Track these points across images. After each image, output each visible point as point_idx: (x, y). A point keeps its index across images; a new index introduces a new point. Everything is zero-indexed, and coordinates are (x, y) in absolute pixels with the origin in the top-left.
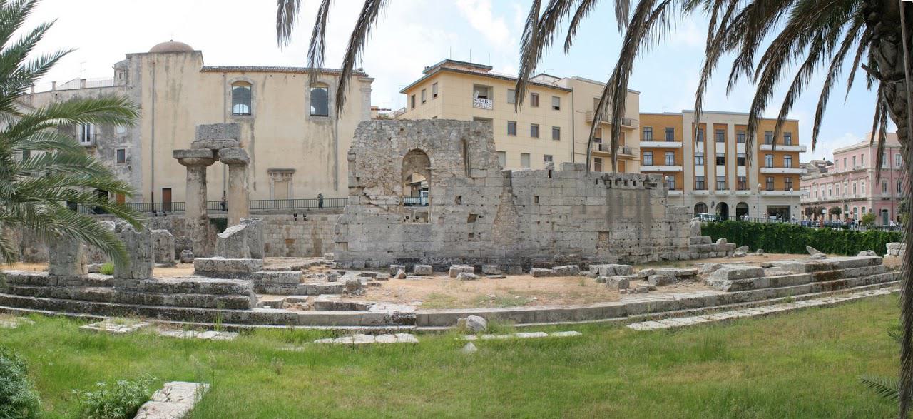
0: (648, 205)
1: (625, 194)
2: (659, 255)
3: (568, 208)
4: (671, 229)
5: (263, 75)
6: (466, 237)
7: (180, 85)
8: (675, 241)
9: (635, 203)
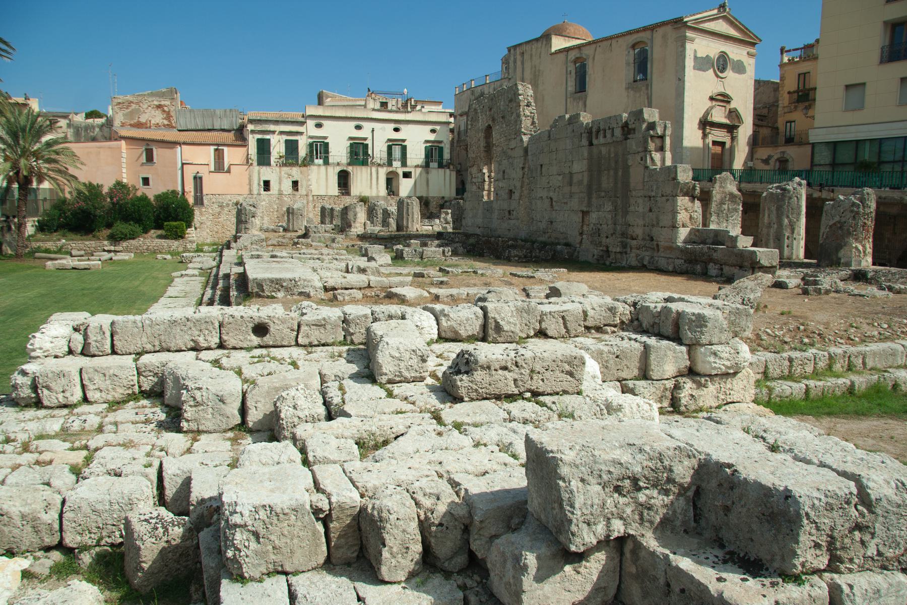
0: (626, 168)
1: (604, 150)
2: (637, 256)
3: (560, 178)
4: (650, 210)
5: (594, 46)
6: (507, 213)
7: (539, 70)
8: (655, 232)
9: (613, 165)
